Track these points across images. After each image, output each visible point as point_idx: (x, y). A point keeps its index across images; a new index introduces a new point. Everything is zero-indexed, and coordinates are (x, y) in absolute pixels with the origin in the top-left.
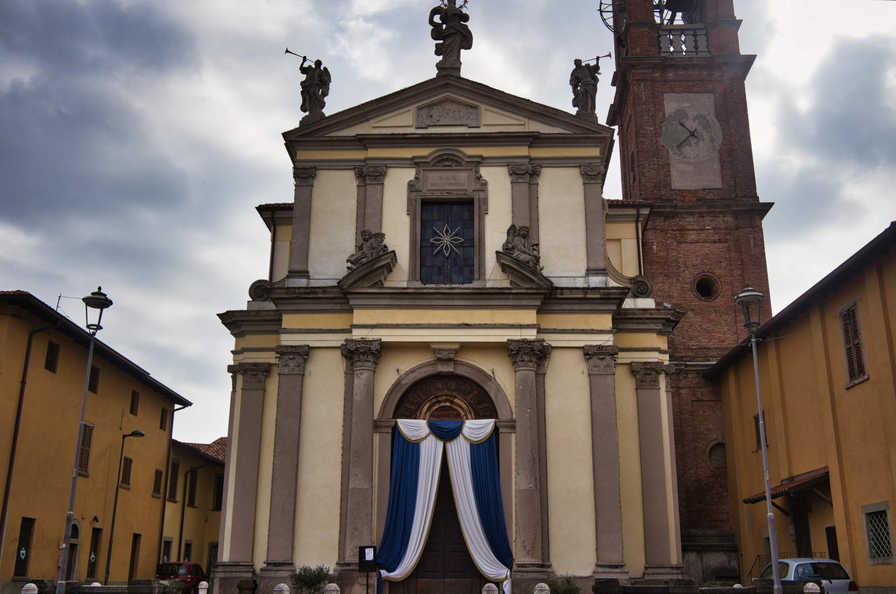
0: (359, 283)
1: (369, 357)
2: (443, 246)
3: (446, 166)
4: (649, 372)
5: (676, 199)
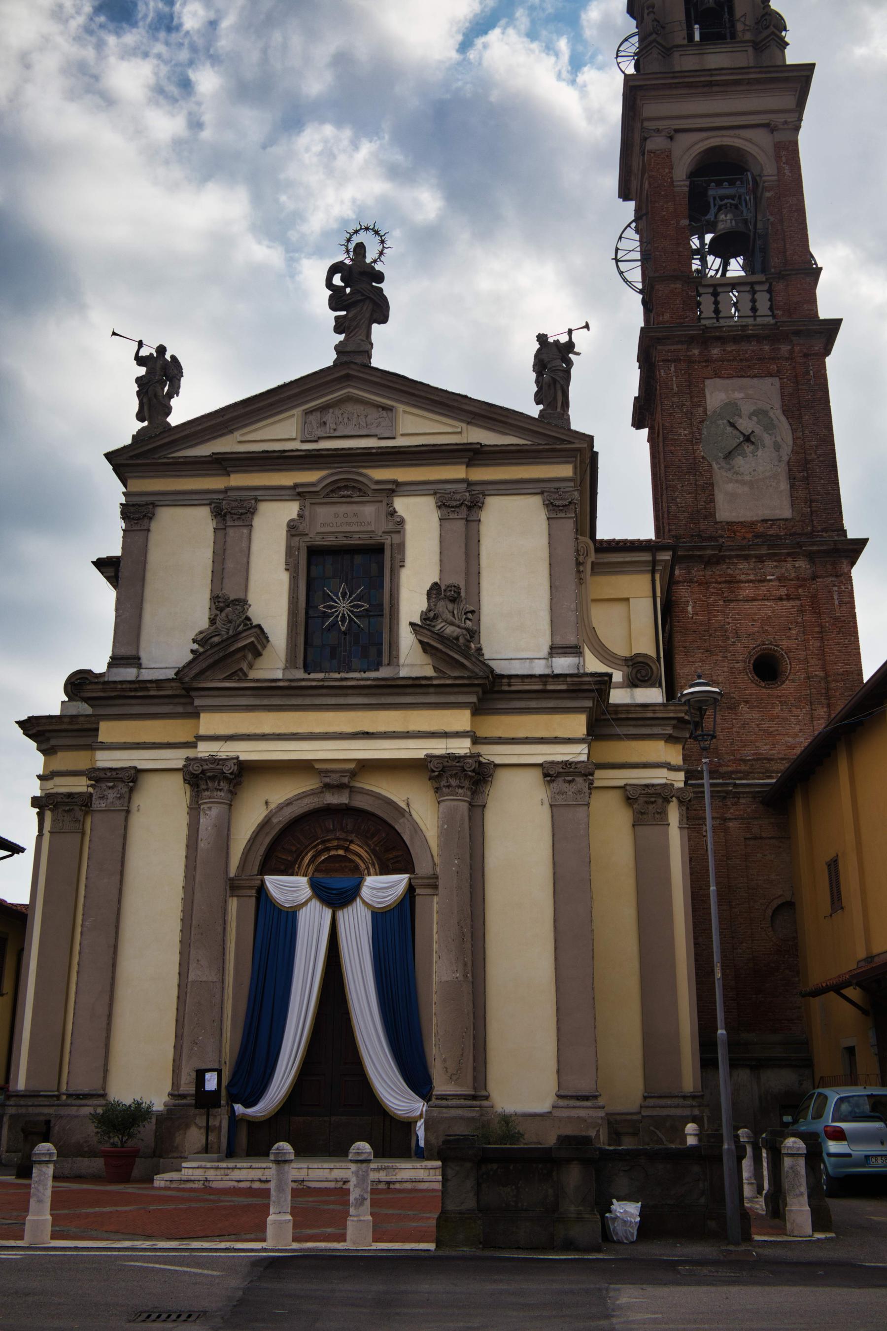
0: (208, 673)
1: (222, 783)
2: (337, 616)
3: (343, 497)
4: (653, 799)
5: (722, 537)
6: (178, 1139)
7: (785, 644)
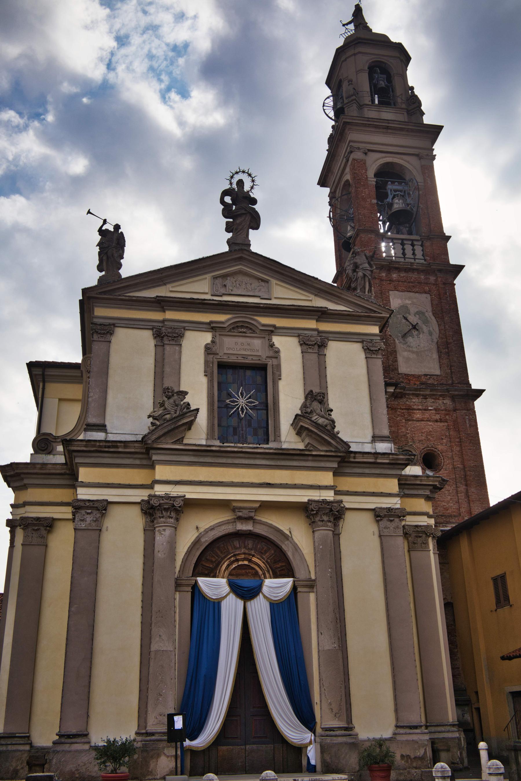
0: (162, 439)
1: (172, 513)
2: (238, 408)
3: (241, 332)
4: (421, 535)
5: (403, 382)
6: (152, 765)
7: (440, 447)
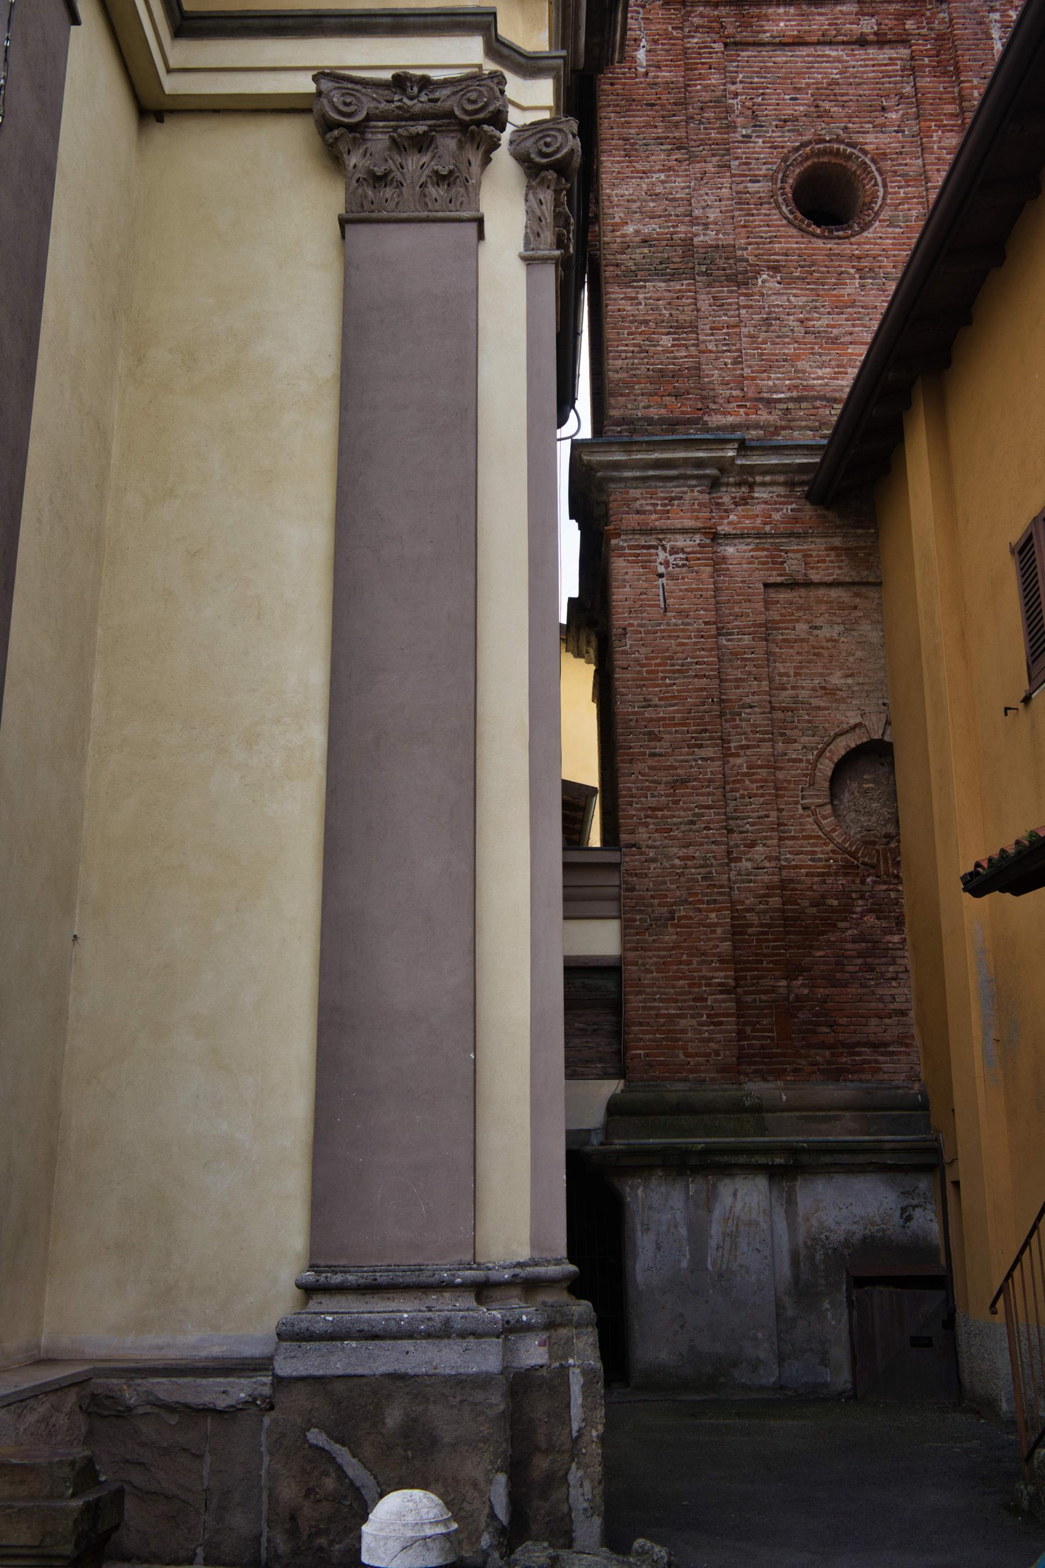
7: (872, 141)
